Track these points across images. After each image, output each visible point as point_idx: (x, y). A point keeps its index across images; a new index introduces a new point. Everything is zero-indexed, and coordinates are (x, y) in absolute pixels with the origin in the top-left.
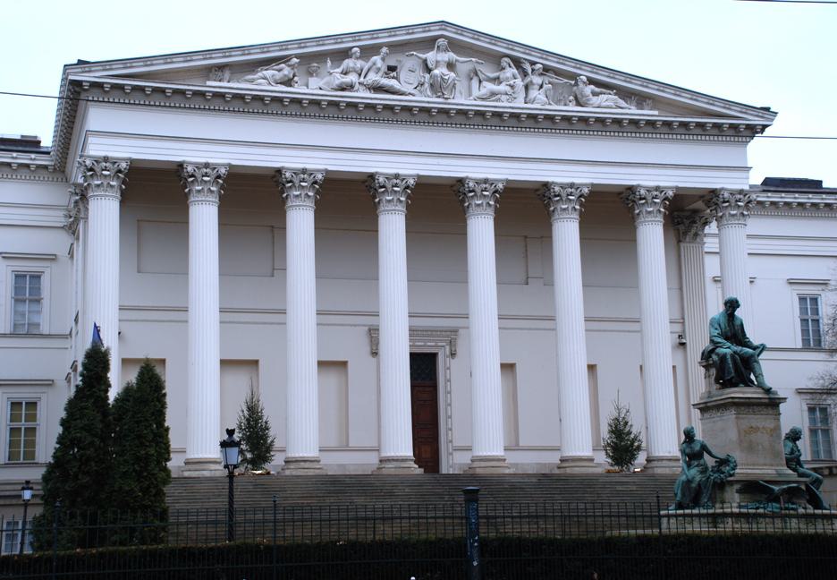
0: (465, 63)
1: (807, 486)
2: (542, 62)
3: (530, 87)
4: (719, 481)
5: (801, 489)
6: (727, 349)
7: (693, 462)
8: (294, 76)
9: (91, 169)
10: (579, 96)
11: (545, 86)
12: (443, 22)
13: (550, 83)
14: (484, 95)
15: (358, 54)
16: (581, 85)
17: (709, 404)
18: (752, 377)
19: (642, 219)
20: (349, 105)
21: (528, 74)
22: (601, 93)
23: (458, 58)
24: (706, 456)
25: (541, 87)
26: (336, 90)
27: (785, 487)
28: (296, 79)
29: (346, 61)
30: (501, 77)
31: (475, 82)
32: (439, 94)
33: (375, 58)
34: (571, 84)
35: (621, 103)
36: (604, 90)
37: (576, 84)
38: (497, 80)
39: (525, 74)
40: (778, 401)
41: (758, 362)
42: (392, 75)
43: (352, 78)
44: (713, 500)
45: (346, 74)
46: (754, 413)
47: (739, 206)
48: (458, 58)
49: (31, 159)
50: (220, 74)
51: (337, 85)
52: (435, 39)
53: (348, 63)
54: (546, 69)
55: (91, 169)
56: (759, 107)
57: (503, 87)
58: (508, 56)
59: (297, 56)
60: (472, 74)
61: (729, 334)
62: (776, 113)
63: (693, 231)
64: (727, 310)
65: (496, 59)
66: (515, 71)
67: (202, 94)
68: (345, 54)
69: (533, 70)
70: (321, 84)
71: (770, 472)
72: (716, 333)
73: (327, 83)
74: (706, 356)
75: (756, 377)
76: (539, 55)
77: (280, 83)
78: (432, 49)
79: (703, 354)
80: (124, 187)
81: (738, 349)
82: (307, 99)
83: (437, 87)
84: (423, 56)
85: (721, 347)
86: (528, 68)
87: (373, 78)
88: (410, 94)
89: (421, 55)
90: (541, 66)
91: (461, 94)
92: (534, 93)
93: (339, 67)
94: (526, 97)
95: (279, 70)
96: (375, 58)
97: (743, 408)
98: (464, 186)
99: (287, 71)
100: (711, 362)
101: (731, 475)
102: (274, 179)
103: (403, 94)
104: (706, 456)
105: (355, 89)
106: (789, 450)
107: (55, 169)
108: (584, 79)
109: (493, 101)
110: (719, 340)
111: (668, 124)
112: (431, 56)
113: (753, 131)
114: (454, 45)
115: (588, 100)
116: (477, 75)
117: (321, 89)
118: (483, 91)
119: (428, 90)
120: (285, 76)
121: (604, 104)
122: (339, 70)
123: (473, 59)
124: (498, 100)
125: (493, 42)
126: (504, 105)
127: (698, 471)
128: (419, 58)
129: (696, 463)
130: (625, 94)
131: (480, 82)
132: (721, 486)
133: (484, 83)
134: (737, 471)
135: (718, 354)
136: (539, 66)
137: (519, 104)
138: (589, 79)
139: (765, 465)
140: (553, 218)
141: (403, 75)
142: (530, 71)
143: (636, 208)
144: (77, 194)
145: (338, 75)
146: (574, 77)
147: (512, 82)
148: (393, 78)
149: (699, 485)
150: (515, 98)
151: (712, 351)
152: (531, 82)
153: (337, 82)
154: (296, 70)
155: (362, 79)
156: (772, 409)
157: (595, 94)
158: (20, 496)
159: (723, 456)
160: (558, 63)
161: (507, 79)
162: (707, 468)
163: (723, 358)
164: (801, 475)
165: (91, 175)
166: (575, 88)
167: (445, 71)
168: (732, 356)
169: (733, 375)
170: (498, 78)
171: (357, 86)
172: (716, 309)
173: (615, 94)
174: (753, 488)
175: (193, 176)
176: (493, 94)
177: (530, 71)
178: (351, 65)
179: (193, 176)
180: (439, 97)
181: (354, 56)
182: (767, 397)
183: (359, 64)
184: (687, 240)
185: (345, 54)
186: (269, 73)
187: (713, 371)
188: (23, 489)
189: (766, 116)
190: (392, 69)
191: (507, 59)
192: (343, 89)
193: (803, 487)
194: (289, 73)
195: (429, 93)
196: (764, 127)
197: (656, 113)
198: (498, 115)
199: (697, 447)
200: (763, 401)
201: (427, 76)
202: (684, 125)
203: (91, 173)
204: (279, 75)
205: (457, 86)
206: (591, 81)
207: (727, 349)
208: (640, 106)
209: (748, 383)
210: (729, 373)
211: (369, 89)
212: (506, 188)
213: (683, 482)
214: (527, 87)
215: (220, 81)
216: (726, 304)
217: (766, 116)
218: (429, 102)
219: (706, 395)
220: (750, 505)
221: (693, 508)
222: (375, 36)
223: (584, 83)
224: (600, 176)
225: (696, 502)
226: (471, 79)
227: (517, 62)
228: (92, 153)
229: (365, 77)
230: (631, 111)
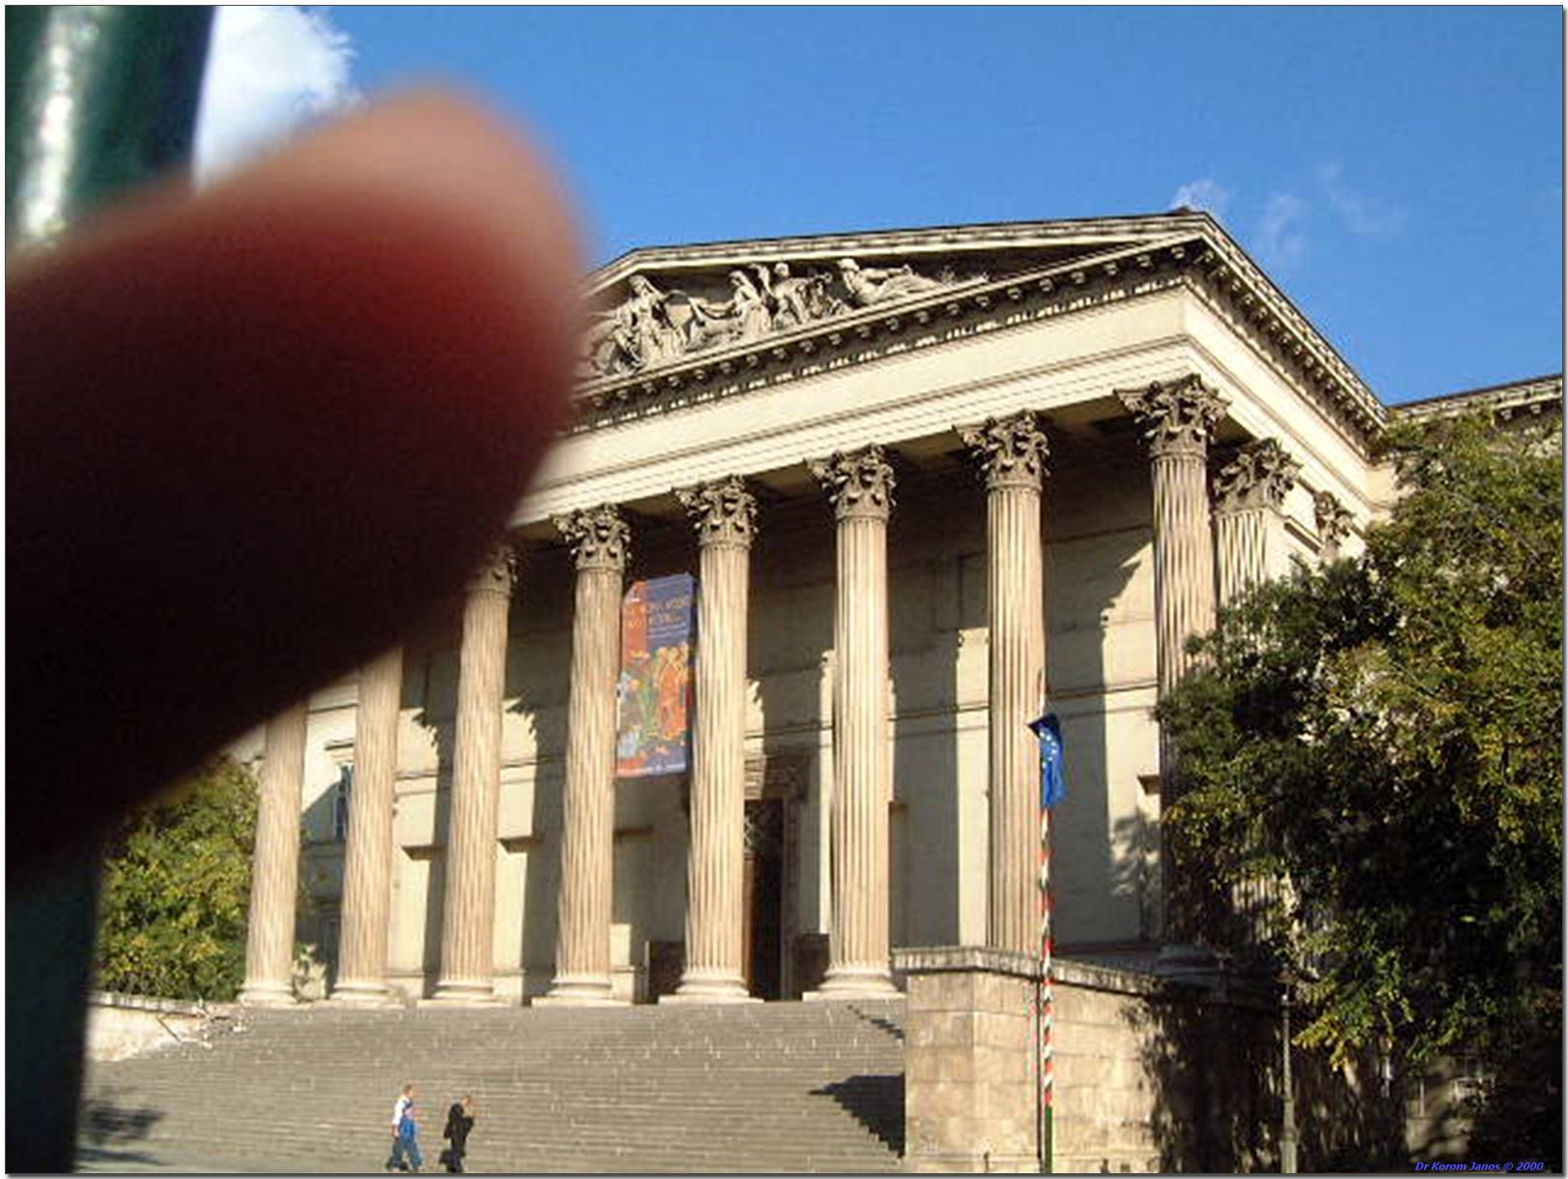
2: (780, 258)
36: (892, 270)
37: (838, 278)
38: (729, 314)
54: (798, 269)
66: (748, 288)
69: (775, 280)
86: (764, 275)
114: (657, 279)
126: (724, 349)
138: (857, 260)
150: (740, 333)
157: (878, 282)
176: (709, 336)
191: (738, 274)
206: (863, 263)
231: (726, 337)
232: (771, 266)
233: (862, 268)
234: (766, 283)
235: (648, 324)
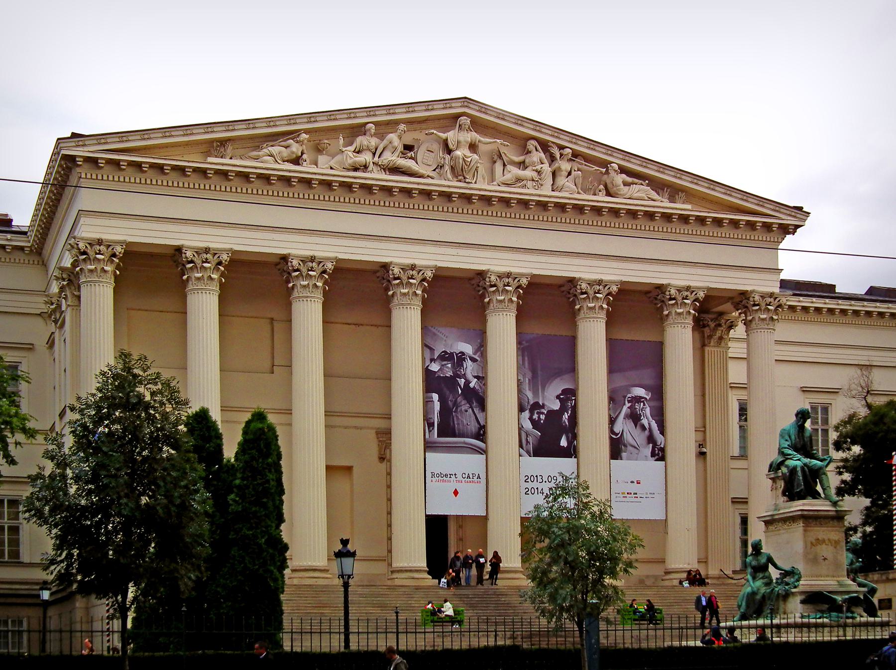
0: (487, 143)
1: (865, 596)
3: (557, 174)
4: (784, 593)
5: (860, 598)
6: (797, 461)
7: (758, 574)
8: (302, 153)
9: (84, 253)
10: (609, 186)
11: (573, 172)
13: (578, 170)
14: (509, 180)
15: (373, 131)
16: (612, 173)
17: (777, 517)
18: (819, 488)
19: (670, 320)
20: (363, 186)
21: (556, 159)
22: (633, 183)
23: (482, 139)
24: (771, 568)
25: (569, 174)
26: (348, 170)
27: (847, 597)
28: (305, 156)
30: (527, 161)
31: (498, 167)
32: (460, 178)
33: (393, 137)
34: (601, 172)
35: (654, 195)
36: (636, 180)
37: (607, 172)
38: (522, 165)
39: (552, 159)
40: (843, 513)
41: (825, 474)
42: (409, 155)
43: (366, 157)
44: (774, 613)
45: (358, 152)
46: (821, 525)
47: (769, 310)
48: (482, 139)
49: (7, 240)
50: (222, 150)
51: (350, 165)
52: (456, 117)
53: (361, 140)
54: (576, 155)
55: (84, 253)
56: (792, 205)
57: (528, 173)
58: (534, 138)
59: (307, 131)
60: (496, 157)
61: (799, 446)
62: (809, 213)
63: (718, 334)
64: (798, 421)
65: (522, 142)
66: (542, 155)
67: (203, 172)
68: (358, 130)
69: (561, 155)
70: (332, 163)
71: (832, 583)
72: (786, 444)
73: (341, 163)
74: (774, 467)
75: (824, 490)
76: (568, 139)
77: (287, 161)
79: (771, 466)
80: (118, 272)
81: (807, 460)
82: (317, 179)
83: (458, 172)
84: (443, 136)
85: (791, 459)
86: (556, 152)
87: (389, 158)
88: (428, 176)
89: (441, 134)
90: (571, 151)
91: (484, 179)
92: (561, 180)
93: (351, 144)
94: (553, 185)
95: (286, 147)
96: (391, 135)
97: (811, 521)
98: (484, 279)
99: (296, 148)
100: (780, 474)
101: (795, 587)
102: (278, 267)
103: (421, 176)
104: (771, 568)
105: (370, 169)
106: (850, 561)
107: (31, 251)
108: (616, 167)
109: (519, 187)
110: (790, 452)
111: (701, 220)
112: (452, 136)
113: (787, 230)
114: (477, 125)
115: (619, 190)
116: (500, 156)
117: (331, 168)
118: (508, 177)
119: (448, 171)
120: (293, 153)
121: (636, 195)
122: (352, 148)
123: (498, 141)
124: (524, 186)
127: (763, 583)
128: (439, 137)
129: (761, 576)
130: (658, 185)
131: (504, 165)
132: (786, 596)
133: (509, 167)
134: (801, 582)
135: (787, 466)
136: (568, 151)
137: (546, 192)
139: (827, 576)
140: (578, 318)
141: (421, 153)
142: (558, 156)
143: (665, 308)
144: (64, 279)
145: (351, 154)
146: (605, 164)
147: (538, 167)
148: (411, 158)
149: (764, 596)
150: (542, 185)
151: (782, 463)
152: (559, 169)
153: (350, 161)
154: (304, 146)
155: (376, 159)
156: (838, 521)
157: (626, 184)
158: (38, 596)
159: (787, 568)
161: (533, 164)
162: (772, 580)
163: (793, 471)
164: (860, 585)
165: (84, 260)
166: (606, 176)
167: (467, 152)
168: (802, 468)
169: (803, 487)
170: (524, 162)
171: (371, 166)
172: (789, 421)
173: (648, 185)
174: (814, 599)
175: (192, 262)
176: (519, 180)
177: (558, 156)
178: (365, 143)
179: (192, 262)
180: (460, 181)
181: (368, 133)
182: (834, 509)
183: (374, 142)
184: (712, 344)
185: (358, 130)
186: (275, 150)
187: (781, 484)
188: (42, 589)
189: (798, 216)
190: (408, 148)
192: (356, 169)
193: (862, 597)
194: (298, 150)
195: (449, 176)
196: (798, 227)
197: (689, 207)
198: (524, 204)
199: (763, 560)
200: (830, 513)
201: (448, 157)
202: (718, 222)
203: (84, 257)
204: (285, 153)
205: (479, 170)
206: (623, 170)
207: (797, 461)
208: (672, 199)
209: (815, 495)
210: (799, 485)
211: (384, 170)
212: (530, 284)
213: (748, 593)
214: (554, 174)
215: (222, 157)
216: (797, 415)
217: (798, 216)
218: (449, 187)
219: (773, 508)
220: (813, 615)
221: (757, 618)
223: (616, 171)
224: (630, 273)
225: (759, 614)
226: (495, 162)
227: (544, 146)
228: (84, 235)
230: (663, 204)
231: (530, 184)
232: (561, 148)
234: (558, 158)
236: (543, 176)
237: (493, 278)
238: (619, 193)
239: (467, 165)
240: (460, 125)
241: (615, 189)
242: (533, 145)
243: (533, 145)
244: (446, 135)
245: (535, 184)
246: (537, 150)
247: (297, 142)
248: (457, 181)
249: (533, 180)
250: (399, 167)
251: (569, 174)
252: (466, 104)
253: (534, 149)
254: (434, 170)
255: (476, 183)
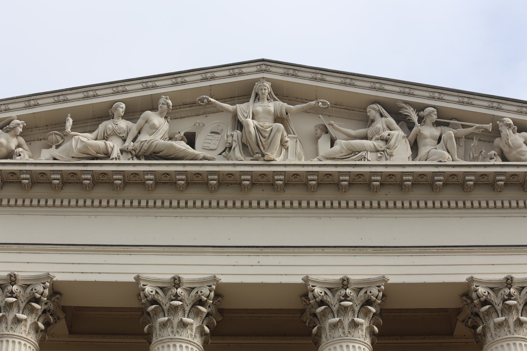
3: (420, 144)
10: (506, 150)
12: (263, 60)
21: (414, 124)
29: (104, 123)
37: (497, 133)
53: (107, 125)
59: (19, 118)
66: (391, 120)
69: (421, 120)
76: (427, 94)
78: (248, 101)
90: (432, 109)
109: (353, 160)
115: (521, 153)
116: (327, 132)
117: (55, 159)
125: (348, 81)
133: (338, 141)
142: (415, 118)
147: (385, 134)
150: (391, 156)
160: (460, 103)
161: (377, 132)
171: (116, 153)
176: (353, 152)
183: (123, 124)
201: (237, 133)
211: (138, 158)
214: (415, 147)
222: (150, 84)
223: (509, 126)
226: (319, 138)
229: (134, 140)
231: (370, 156)
232: (420, 108)
233: (519, 131)
235: (268, 124)
236: (392, 142)
237: (317, 290)
238: (523, 158)
239: (265, 137)
240: (257, 95)
241: (514, 152)
242: (374, 109)
243: (374, 109)
244: (234, 107)
245: (379, 155)
246: (382, 115)
247: (7, 132)
248: (251, 160)
249: (378, 151)
250: (157, 150)
251: (439, 140)
252: (264, 67)
253: (378, 115)
254: (220, 154)
255: (284, 160)
